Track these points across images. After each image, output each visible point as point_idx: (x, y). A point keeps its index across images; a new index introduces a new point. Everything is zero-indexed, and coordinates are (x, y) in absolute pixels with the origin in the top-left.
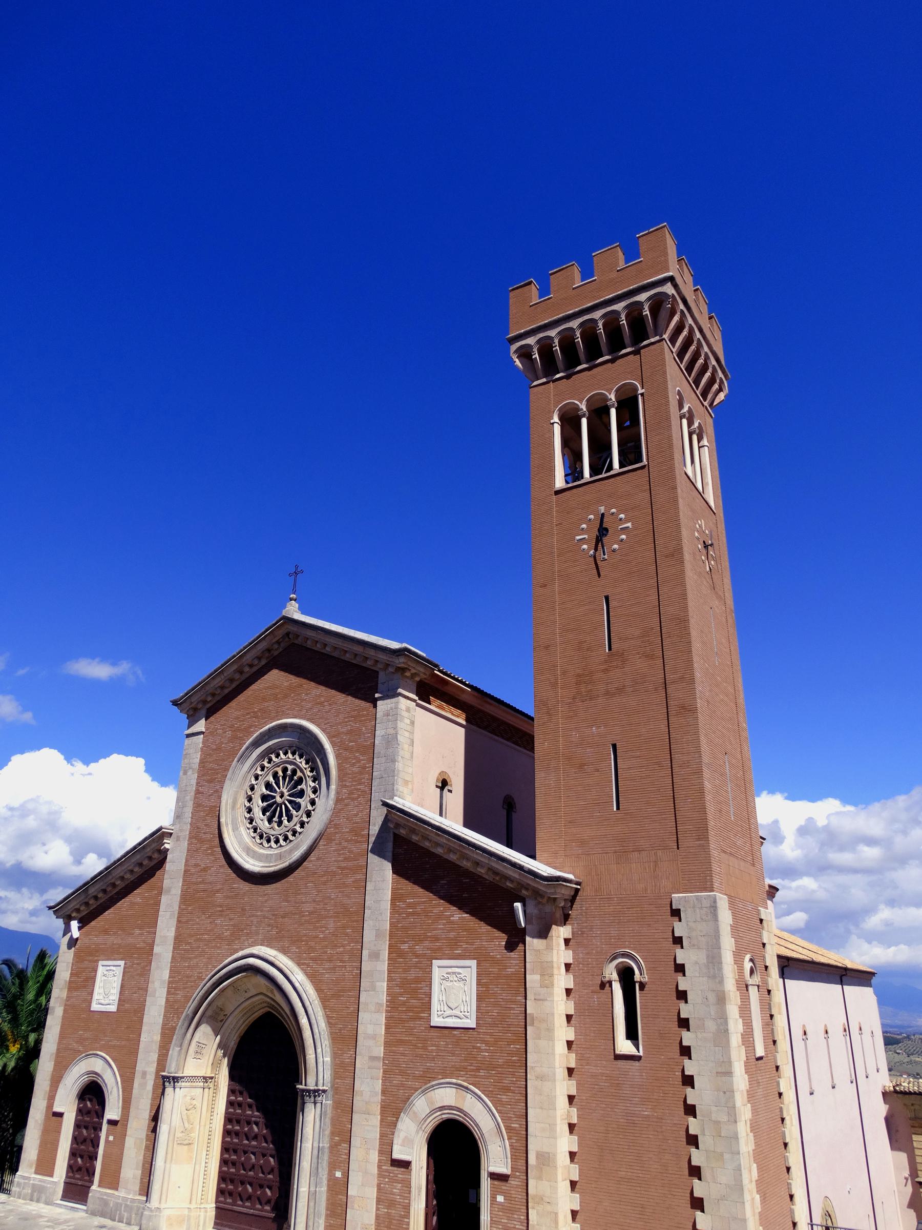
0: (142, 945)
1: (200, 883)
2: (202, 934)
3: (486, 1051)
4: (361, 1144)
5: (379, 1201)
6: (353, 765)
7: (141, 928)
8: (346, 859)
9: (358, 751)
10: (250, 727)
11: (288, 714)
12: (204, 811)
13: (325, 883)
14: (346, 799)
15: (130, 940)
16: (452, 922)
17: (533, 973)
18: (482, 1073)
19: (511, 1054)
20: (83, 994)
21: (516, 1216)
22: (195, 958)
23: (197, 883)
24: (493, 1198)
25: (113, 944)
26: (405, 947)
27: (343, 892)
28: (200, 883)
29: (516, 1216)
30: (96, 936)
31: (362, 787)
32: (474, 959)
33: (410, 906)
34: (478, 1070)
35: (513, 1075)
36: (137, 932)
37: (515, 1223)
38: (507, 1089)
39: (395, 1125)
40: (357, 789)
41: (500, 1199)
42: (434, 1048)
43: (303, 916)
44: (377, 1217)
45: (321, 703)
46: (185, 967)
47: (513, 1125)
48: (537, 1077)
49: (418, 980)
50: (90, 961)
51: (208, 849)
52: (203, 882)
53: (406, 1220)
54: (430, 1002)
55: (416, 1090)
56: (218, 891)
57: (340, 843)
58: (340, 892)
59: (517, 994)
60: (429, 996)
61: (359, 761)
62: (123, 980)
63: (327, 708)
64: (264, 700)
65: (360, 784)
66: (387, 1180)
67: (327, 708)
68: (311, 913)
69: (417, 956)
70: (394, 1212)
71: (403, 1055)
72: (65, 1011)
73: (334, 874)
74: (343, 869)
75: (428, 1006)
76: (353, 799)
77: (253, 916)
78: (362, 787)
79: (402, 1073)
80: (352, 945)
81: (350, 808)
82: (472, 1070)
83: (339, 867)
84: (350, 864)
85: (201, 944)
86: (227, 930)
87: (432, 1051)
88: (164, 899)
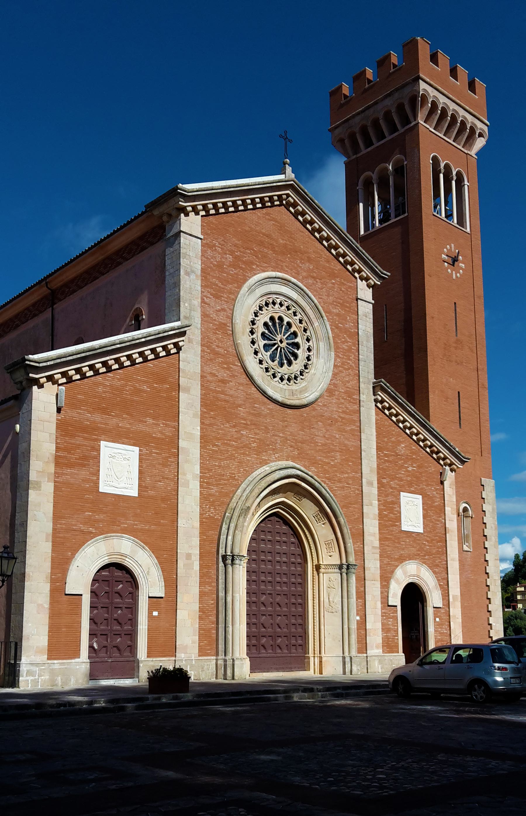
0: (159, 435)
2: (230, 440)
3: (428, 546)
6: (343, 343)
8: (344, 412)
10: (253, 264)
11: (287, 271)
15: (141, 427)
16: (408, 471)
18: (427, 557)
19: (438, 548)
20: (84, 473)
24: (435, 619)
25: (118, 426)
26: (384, 481)
27: (344, 435)
30: (89, 412)
32: (420, 495)
34: (425, 556)
35: (439, 558)
36: (150, 421)
38: (437, 566)
39: (388, 588)
42: (404, 543)
43: (318, 446)
46: (215, 465)
49: (393, 503)
50: (85, 438)
52: (223, 392)
54: (400, 517)
55: (397, 566)
56: (240, 406)
59: (440, 517)
61: (347, 342)
62: (140, 466)
67: (319, 285)
68: (323, 445)
69: (392, 488)
71: (388, 546)
72: (56, 489)
73: (336, 421)
74: (343, 418)
75: (399, 519)
77: (276, 436)
79: (388, 557)
80: (353, 473)
81: (343, 375)
82: (422, 556)
83: (340, 417)
86: (255, 442)
87: (402, 545)
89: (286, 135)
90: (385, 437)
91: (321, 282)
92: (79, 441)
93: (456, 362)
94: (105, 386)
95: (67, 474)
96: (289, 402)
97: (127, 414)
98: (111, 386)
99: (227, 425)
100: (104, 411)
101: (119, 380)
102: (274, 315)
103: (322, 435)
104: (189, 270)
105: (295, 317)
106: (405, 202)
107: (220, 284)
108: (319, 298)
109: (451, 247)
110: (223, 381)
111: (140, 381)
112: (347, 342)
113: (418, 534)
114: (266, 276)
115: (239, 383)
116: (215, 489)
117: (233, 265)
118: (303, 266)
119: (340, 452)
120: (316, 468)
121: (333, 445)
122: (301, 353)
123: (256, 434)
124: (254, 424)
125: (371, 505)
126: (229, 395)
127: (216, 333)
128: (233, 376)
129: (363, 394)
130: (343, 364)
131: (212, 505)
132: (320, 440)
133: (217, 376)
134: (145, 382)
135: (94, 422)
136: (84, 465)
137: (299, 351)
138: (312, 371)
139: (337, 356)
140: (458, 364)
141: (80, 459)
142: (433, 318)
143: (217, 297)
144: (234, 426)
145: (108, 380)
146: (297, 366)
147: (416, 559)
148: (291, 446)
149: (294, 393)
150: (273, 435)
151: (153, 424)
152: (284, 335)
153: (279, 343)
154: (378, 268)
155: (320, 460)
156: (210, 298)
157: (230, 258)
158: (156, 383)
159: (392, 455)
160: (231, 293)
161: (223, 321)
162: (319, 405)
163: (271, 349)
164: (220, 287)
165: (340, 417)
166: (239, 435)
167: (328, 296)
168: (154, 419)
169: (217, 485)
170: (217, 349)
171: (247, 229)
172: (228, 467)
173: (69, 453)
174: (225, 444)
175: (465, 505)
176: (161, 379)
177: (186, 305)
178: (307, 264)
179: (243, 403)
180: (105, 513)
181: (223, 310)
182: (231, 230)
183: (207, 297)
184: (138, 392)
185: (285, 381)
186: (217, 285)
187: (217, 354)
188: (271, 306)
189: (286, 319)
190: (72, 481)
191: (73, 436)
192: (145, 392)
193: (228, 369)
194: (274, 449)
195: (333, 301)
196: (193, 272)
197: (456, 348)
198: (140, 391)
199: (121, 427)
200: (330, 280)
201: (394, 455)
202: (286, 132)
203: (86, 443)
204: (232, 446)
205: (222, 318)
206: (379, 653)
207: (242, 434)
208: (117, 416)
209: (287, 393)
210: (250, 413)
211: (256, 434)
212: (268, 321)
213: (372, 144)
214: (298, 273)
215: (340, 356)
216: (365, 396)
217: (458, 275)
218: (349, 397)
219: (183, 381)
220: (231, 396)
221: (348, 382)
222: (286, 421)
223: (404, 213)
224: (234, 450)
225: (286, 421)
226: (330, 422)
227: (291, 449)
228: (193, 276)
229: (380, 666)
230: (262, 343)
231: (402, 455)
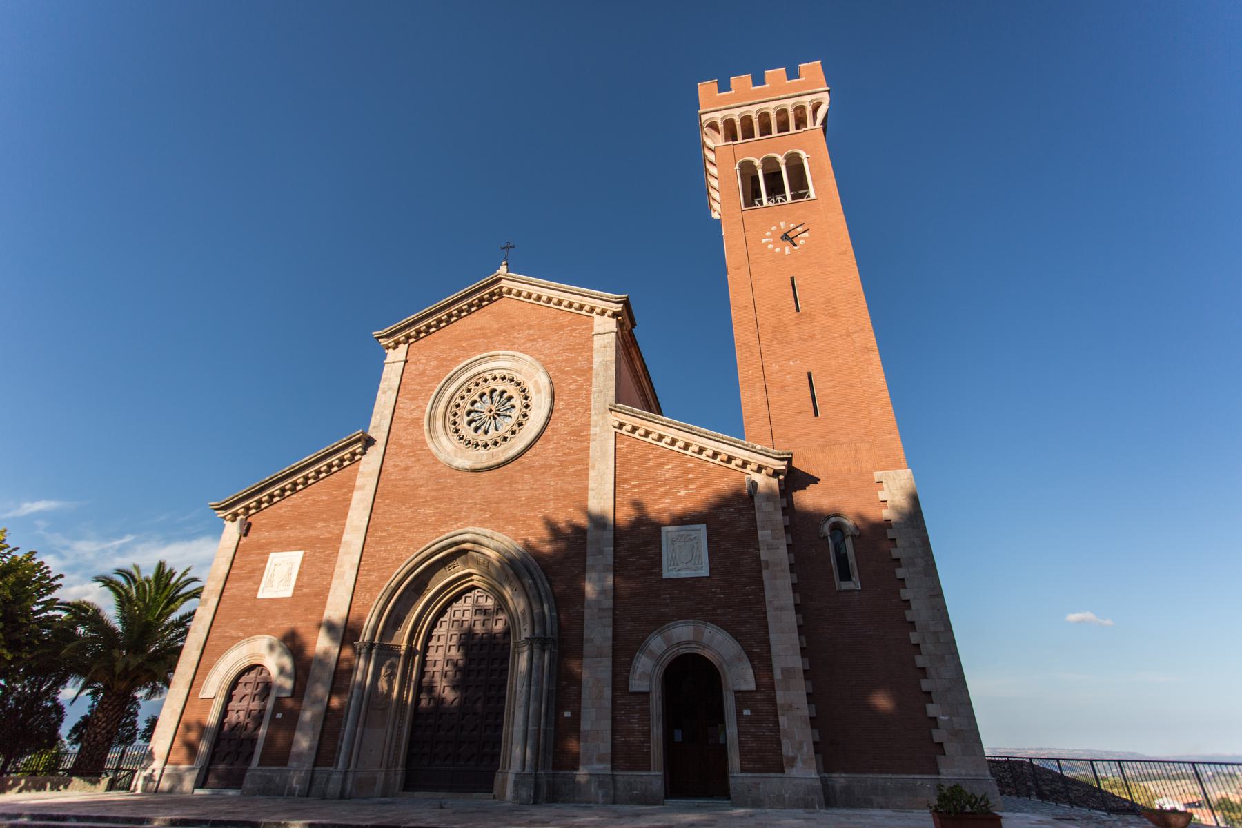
0: (327, 535)
1: (401, 480)
3: (721, 594)
4: (593, 684)
5: (614, 732)
6: (571, 384)
7: (325, 521)
8: (565, 454)
9: (574, 374)
10: (459, 357)
12: (405, 423)
13: (543, 474)
14: (564, 409)
15: (312, 532)
16: (680, 497)
17: (763, 528)
18: (719, 611)
21: (764, 725)
22: (394, 542)
23: (396, 480)
25: (290, 537)
27: (563, 480)
28: (401, 480)
29: (764, 725)
30: (268, 532)
31: (580, 400)
32: (703, 523)
33: (634, 486)
36: (321, 524)
37: (764, 731)
40: (576, 402)
41: (747, 712)
42: (668, 596)
43: (520, 501)
44: (613, 746)
45: (534, 340)
47: (754, 650)
48: (776, 609)
51: (409, 452)
53: (646, 745)
56: (421, 486)
57: (558, 443)
58: (559, 480)
60: (660, 555)
61: (576, 381)
62: (301, 568)
63: (541, 343)
64: (473, 338)
65: (578, 398)
66: (623, 712)
67: (541, 343)
68: (527, 498)
70: (632, 739)
73: (552, 466)
76: (571, 409)
77: (462, 504)
78: (580, 400)
83: (558, 461)
84: (570, 458)
85: (401, 530)
86: (431, 517)
88: (356, 495)
90: (634, 464)
92: (253, 557)
95: (233, 588)
96: (478, 466)
99: (403, 508)
103: (528, 488)
107: (419, 388)
110: (407, 469)
111: (320, 493)
116: (376, 574)
118: (520, 336)
119: (556, 499)
120: (514, 525)
121: (544, 494)
123: (436, 508)
124: (435, 499)
125: (601, 552)
126: (410, 480)
128: (419, 460)
131: (368, 592)
132: (524, 495)
134: (324, 493)
136: (250, 577)
141: (249, 572)
144: (411, 507)
147: (693, 617)
148: (481, 510)
149: (494, 454)
150: (458, 504)
151: (324, 527)
153: (492, 413)
155: (521, 516)
157: (434, 363)
158: (334, 491)
159: (644, 485)
160: (429, 390)
161: (416, 417)
162: (528, 457)
165: (558, 461)
167: (552, 348)
169: (379, 570)
170: (404, 442)
171: (457, 332)
172: (396, 548)
174: (396, 527)
176: (340, 486)
180: (257, 617)
182: (440, 341)
192: (323, 501)
193: (414, 456)
194: (457, 519)
198: (318, 501)
199: (293, 537)
201: (650, 483)
203: (258, 558)
205: (415, 415)
206: (605, 769)
207: (419, 513)
208: (291, 528)
211: (436, 508)
214: (514, 344)
215: (564, 398)
218: (574, 436)
220: (413, 480)
222: (479, 485)
224: (405, 531)
225: (479, 485)
226: (543, 470)
227: (482, 513)
229: (600, 793)
231: (666, 479)
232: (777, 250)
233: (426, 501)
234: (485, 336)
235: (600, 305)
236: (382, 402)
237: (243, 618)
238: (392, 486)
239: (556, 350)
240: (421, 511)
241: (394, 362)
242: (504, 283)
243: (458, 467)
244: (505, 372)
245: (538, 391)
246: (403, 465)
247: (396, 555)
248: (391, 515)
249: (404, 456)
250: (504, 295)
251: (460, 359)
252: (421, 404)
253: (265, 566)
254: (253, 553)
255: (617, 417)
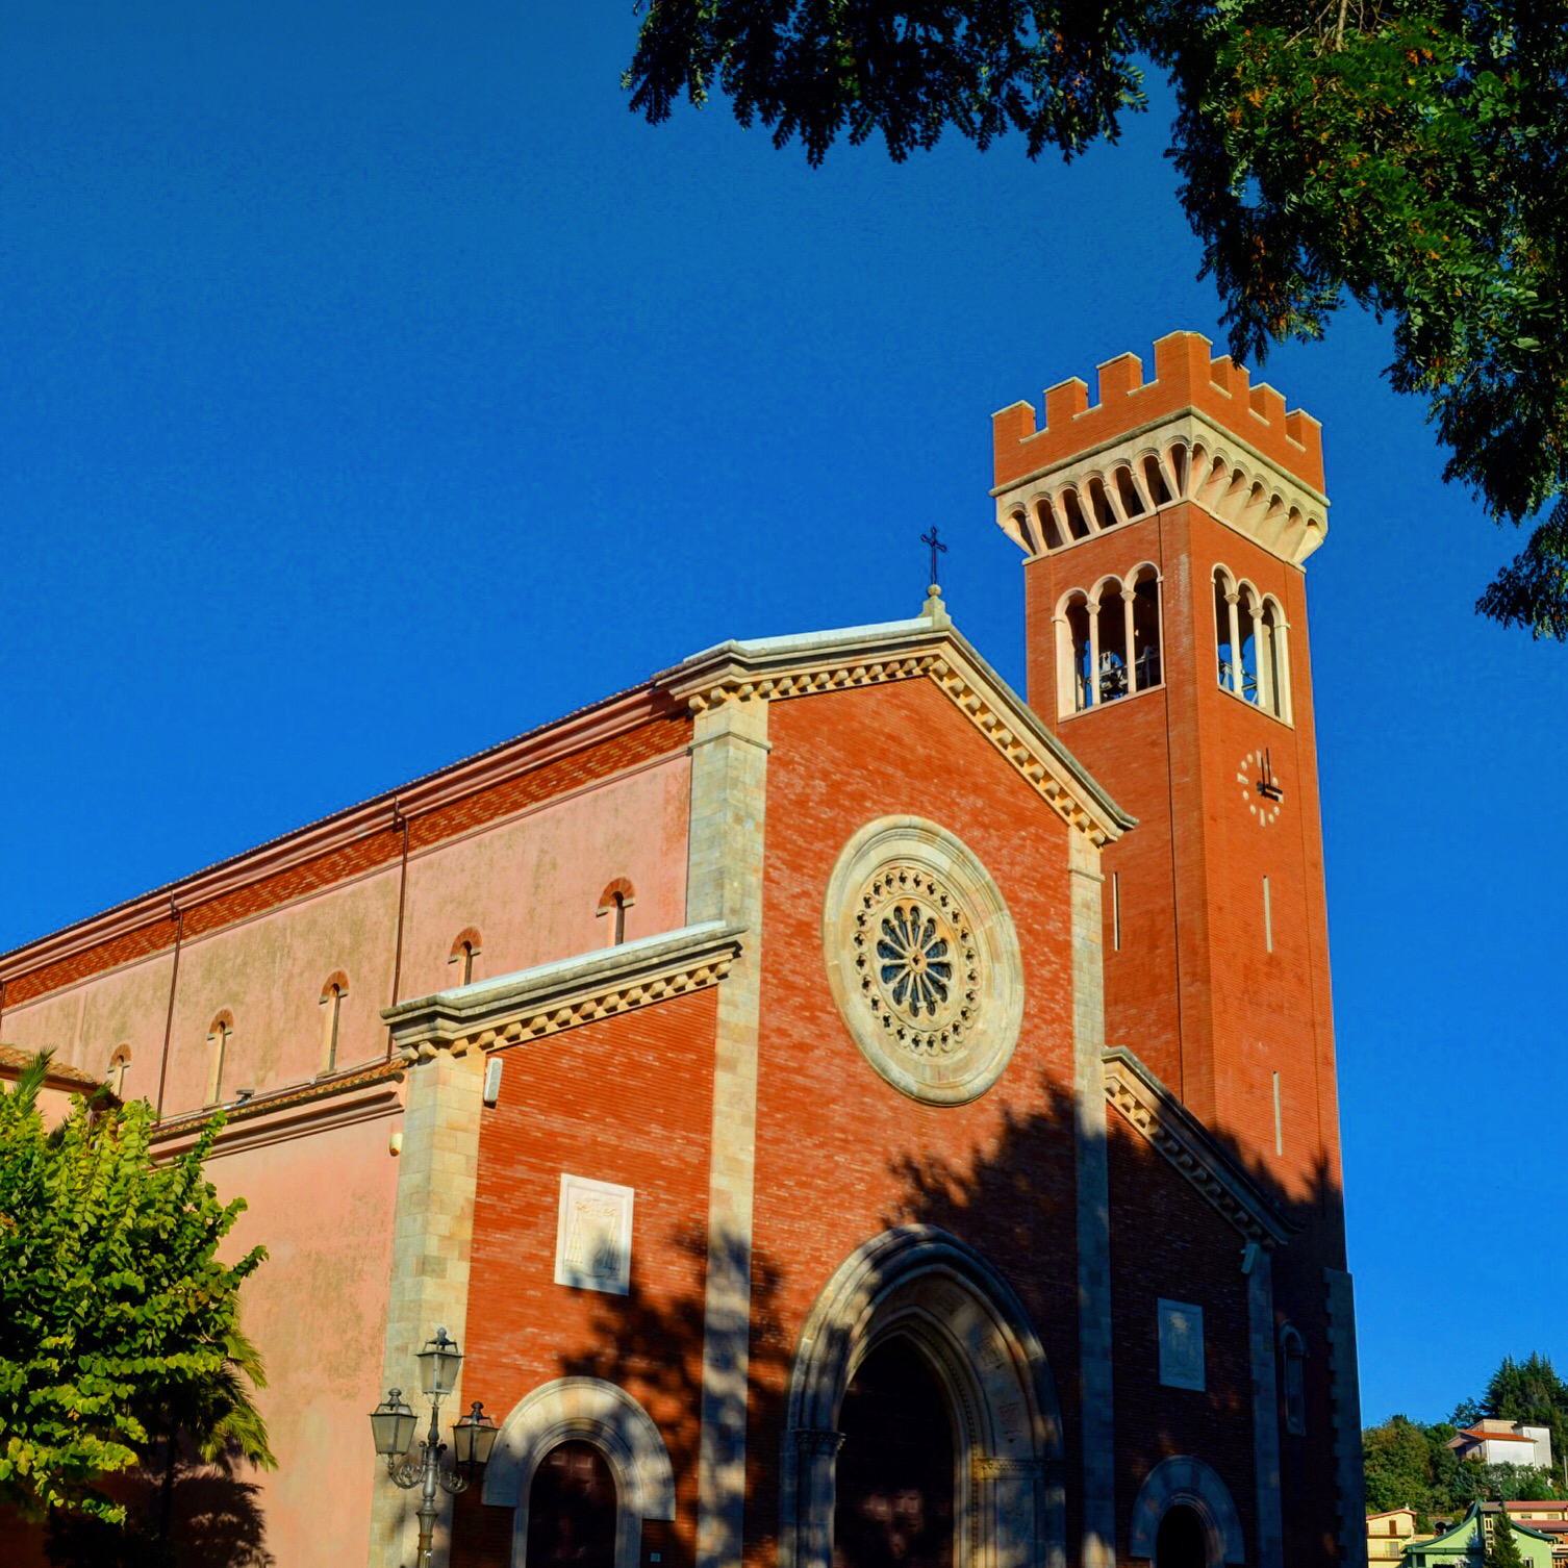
0: (674, 1163)
2: (813, 1176)
6: (1042, 964)
7: (667, 1124)
11: (931, 813)
15: (638, 1144)
20: (525, 1243)
22: (802, 1218)
25: (595, 1143)
30: (542, 1111)
36: (656, 1130)
50: (532, 1167)
51: (803, 1007)
52: (800, 1071)
56: (834, 1100)
62: (635, 1229)
67: (995, 842)
72: (475, 1275)
86: (861, 1180)
88: (722, 1080)
89: (934, 534)
91: (998, 836)
92: (521, 1172)
93: (1269, 1006)
94: (575, 1055)
96: (932, 1094)
97: (616, 1116)
98: (585, 1056)
99: (809, 1142)
100: (570, 1110)
101: (601, 1042)
102: (903, 904)
104: (742, 813)
105: (944, 909)
106: (1159, 658)
107: (801, 842)
108: (995, 869)
109: (1255, 759)
110: (803, 1047)
111: (640, 1044)
112: (1049, 962)
113: (1193, 1394)
114: (892, 825)
115: (832, 1051)
117: (830, 802)
118: (962, 802)
122: (955, 985)
123: (865, 1162)
126: (812, 1077)
127: (792, 945)
128: (822, 1036)
129: (1082, 1077)
130: (1042, 1010)
133: (790, 1036)
135: (552, 1134)
136: (527, 1225)
137: (952, 980)
138: (980, 1026)
139: (1029, 994)
140: (1274, 1011)
142: (1220, 909)
143: (796, 868)
144: (821, 1146)
145: (579, 1044)
146: (947, 1014)
152: (922, 947)
153: (913, 964)
154: (1116, 809)
156: (779, 869)
157: (821, 786)
160: (821, 859)
161: (805, 919)
163: (896, 976)
164: (800, 847)
166: (832, 1165)
167: (1012, 864)
168: (665, 1127)
170: (792, 978)
171: (855, 725)
172: (807, 1235)
173: (501, 1198)
175: (1293, 1330)
177: (736, 884)
178: (972, 798)
179: (840, 1093)
180: (564, 1330)
181: (805, 894)
182: (825, 728)
183: (776, 868)
184: (634, 1068)
185: (923, 1046)
186: (794, 843)
187: (790, 987)
188: (896, 883)
189: (926, 913)
190: (504, 1257)
191: (510, 1162)
192: (649, 1068)
193: (813, 1019)
195: (1023, 876)
196: (750, 816)
197: (1269, 975)
200: (1018, 830)
202: (934, 531)
203: (533, 1176)
204: (817, 1188)
205: (802, 911)
207: (837, 1164)
208: (594, 1120)
209: (928, 1074)
210: (854, 1117)
211: (865, 1162)
212: (891, 916)
213: (1086, 532)
216: (1085, 1082)
217: (1271, 817)
219: (723, 1047)
221: (1051, 1050)
223: (1157, 681)
228: (750, 825)
230: (878, 963)
232: (1246, 795)
233: (846, 1141)
234: (904, 764)
235: (1093, 810)
236: (739, 846)
237: (534, 1326)
238: (783, 1081)
239: (1018, 870)
240: (840, 1158)
241: (748, 741)
242: (945, 649)
243: (898, 1084)
244: (935, 875)
245: (995, 956)
246: (796, 1037)
247: (813, 1249)
248: (791, 1152)
249: (794, 1013)
250: (931, 674)
251: (868, 804)
252: (809, 887)
253: (557, 1201)
254: (520, 1162)
255: (1121, 1075)
